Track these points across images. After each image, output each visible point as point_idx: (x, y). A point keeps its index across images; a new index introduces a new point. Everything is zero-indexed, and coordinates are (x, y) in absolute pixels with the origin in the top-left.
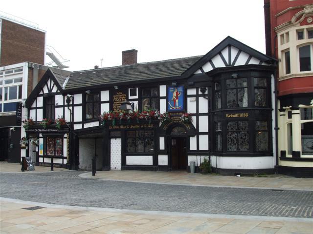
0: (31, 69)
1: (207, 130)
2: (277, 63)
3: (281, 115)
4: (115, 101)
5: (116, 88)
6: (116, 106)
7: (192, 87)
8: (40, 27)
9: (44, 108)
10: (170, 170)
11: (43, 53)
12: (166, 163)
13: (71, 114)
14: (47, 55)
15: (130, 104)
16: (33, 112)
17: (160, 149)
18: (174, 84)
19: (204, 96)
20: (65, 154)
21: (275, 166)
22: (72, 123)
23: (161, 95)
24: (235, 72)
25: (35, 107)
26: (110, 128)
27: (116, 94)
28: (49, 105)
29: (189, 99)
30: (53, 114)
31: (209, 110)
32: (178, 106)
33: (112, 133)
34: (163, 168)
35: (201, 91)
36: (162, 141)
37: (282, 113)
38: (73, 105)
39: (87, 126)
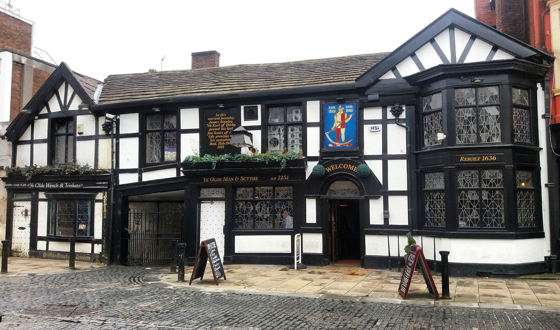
7: (373, 104)
13: (113, 153)
19: (397, 121)
20: (98, 234)
29: (367, 128)
33: (205, 192)
38: (118, 136)
39: (148, 177)
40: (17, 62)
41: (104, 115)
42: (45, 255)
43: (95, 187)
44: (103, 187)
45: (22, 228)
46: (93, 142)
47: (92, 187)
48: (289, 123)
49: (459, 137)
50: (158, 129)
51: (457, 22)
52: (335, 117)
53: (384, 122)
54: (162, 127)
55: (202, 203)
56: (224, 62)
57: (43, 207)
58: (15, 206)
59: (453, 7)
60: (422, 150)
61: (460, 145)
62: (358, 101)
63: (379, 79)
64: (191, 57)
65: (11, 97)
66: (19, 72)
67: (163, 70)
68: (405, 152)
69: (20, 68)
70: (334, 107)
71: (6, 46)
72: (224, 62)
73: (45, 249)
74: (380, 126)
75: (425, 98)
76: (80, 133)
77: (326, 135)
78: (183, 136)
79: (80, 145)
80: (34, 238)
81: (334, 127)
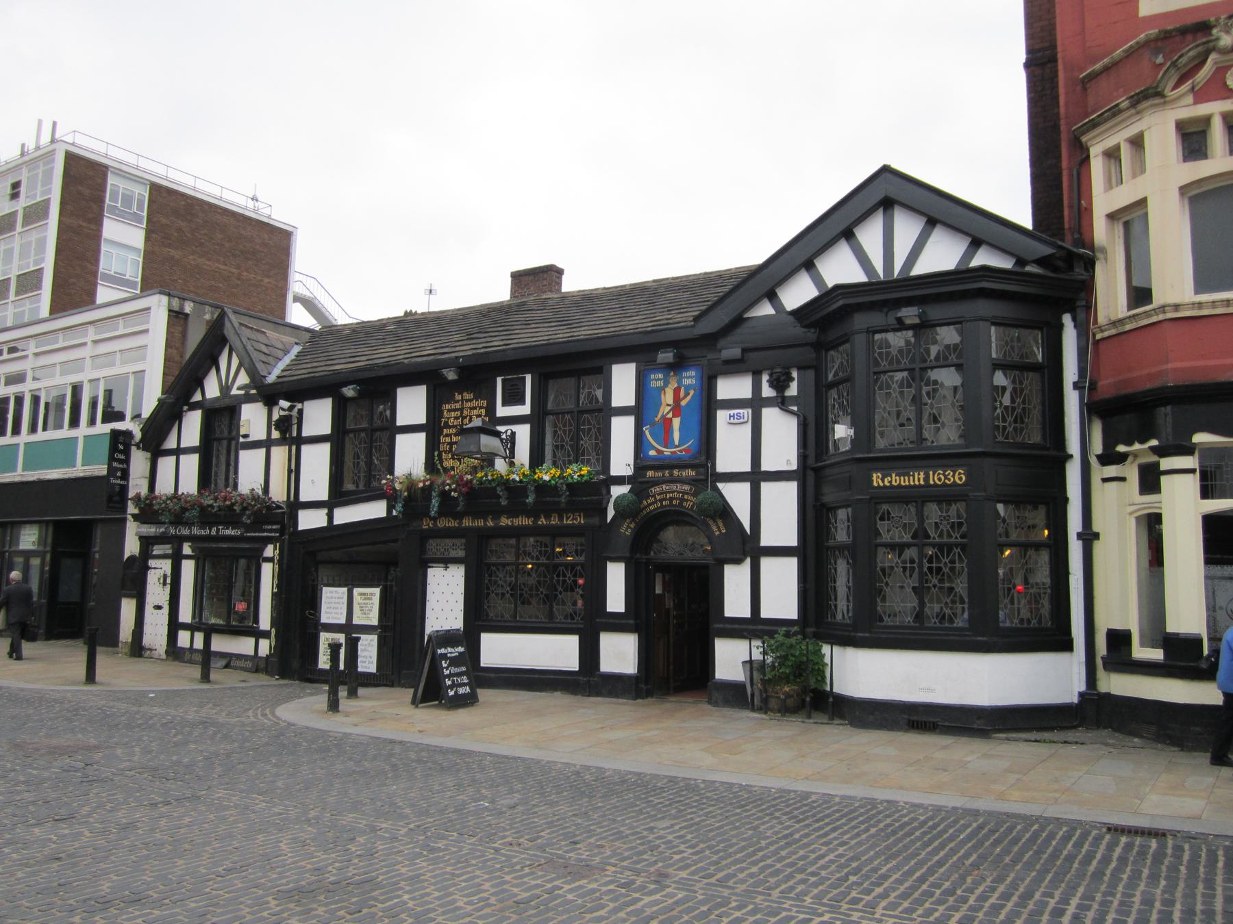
0: (177, 317)
2: (1090, 264)
3: (1105, 480)
4: (447, 426)
5: (451, 375)
6: (451, 444)
7: (733, 368)
8: (279, 215)
9: (206, 450)
10: (648, 694)
11: (284, 296)
13: (290, 471)
14: (298, 304)
15: (497, 434)
16: (166, 465)
17: (609, 609)
18: (666, 356)
19: (782, 402)
20: (265, 623)
21: (1081, 695)
22: (295, 505)
23: (616, 402)
24: (909, 302)
25: (174, 446)
26: (426, 524)
27: (451, 399)
28: (219, 440)
29: (722, 416)
30: (232, 466)
31: (803, 457)
32: (682, 442)
33: (434, 546)
34: (615, 686)
35: (772, 384)
36: (616, 575)
37: (1111, 471)
38: (300, 441)
39: (346, 515)
40: (176, 312)
41: (277, 404)
42: (187, 654)
43: (261, 534)
44: (273, 534)
45: (159, 607)
46: (263, 451)
47: (257, 534)
48: (582, 409)
49: (882, 434)
50: (364, 425)
51: (893, 194)
52: (662, 396)
53: (756, 404)
54: (371, 420)
55: (430, 567)
56: (569, 285)
57: (188, 568)
58: (151, 568)
59: (888, 163)
60: (825, 461)
61: (881, 451)
62: (704, 361)
63: (745, 316)
64: (509, 280)
65: (164, 374)
66: (180, 329)
67: (431, 310)
68: (794, 467)
69: (182, 322)
70: (661, 376)
71: (245, 274)
72: (569, 285)
73: (188, 645)
74: (747, 413)
75: (832, 353)
76: (246, 436)
78: (401, 439)
79: (244, 455)
80: (174, 625)
81: (659, 416)
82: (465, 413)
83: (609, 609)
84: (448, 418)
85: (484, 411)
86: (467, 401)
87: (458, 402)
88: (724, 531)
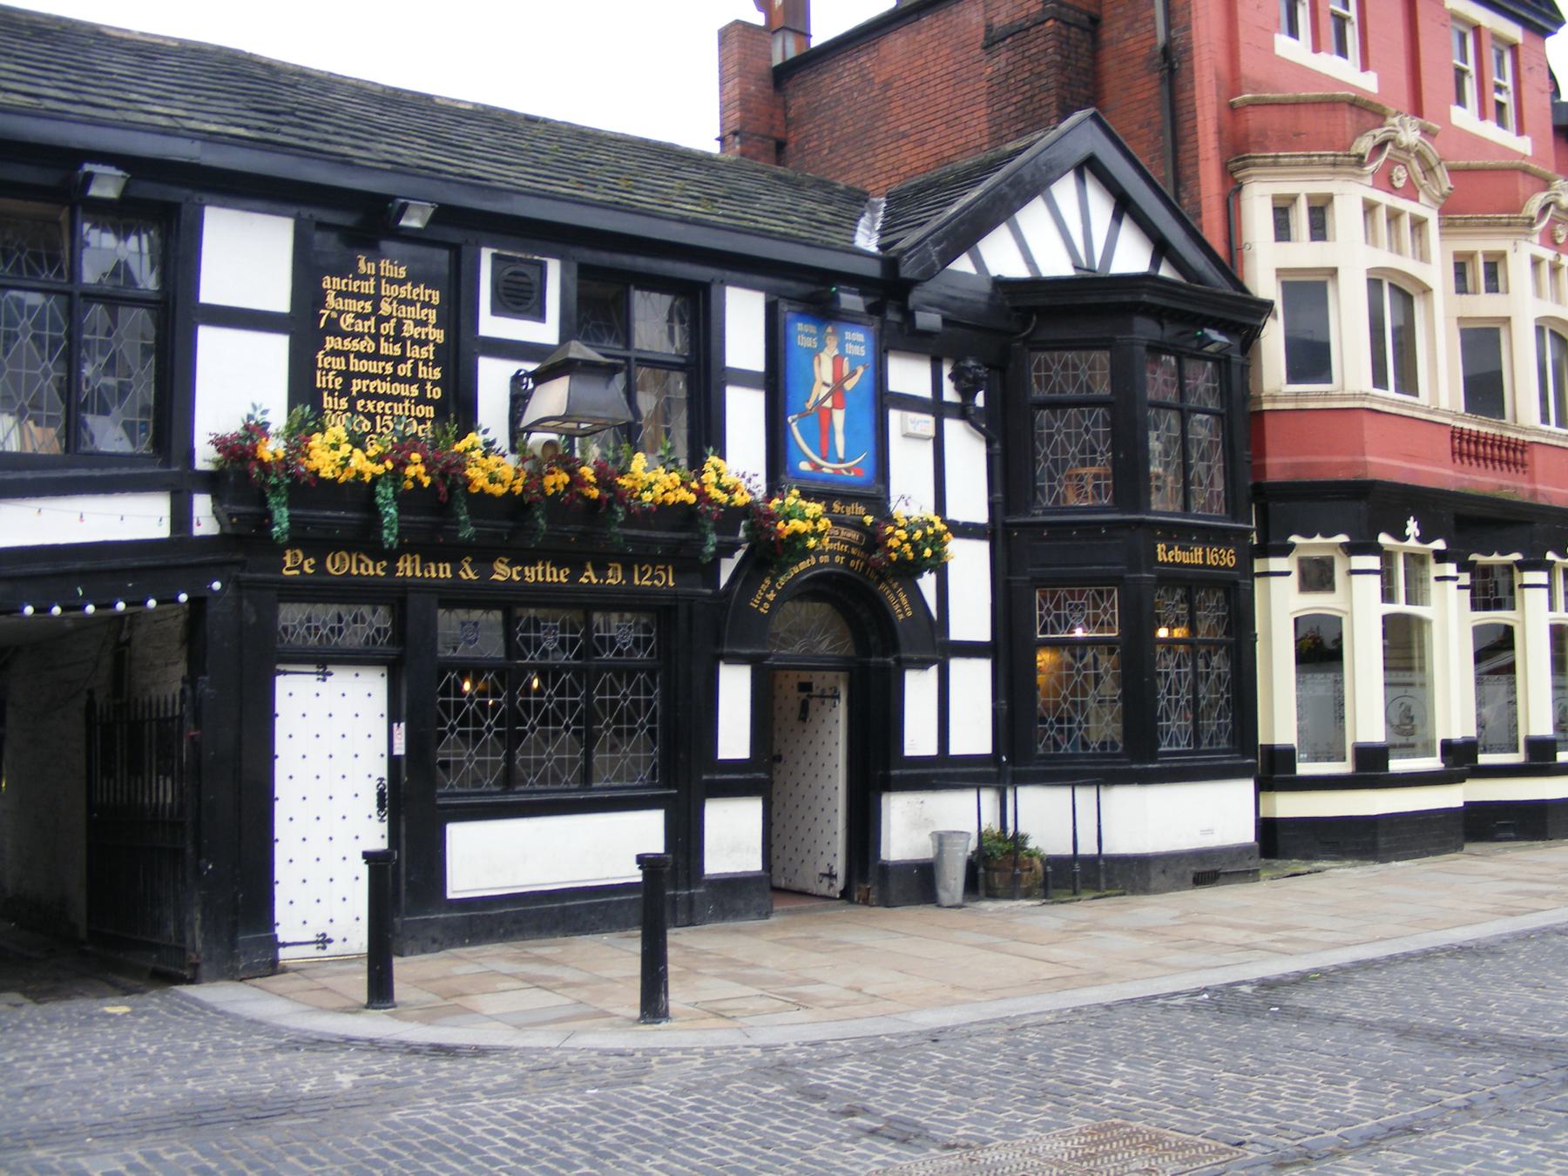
1: (982, 633)
4: (334, 328)
6: (348, 376)
12: (749, 860)
17: (908, 752)
19: (963, 412)
55: (285, 673)
60: (1034, 515)
77: (790, 425)
82: (385, 309)
83: (908, 752)
84: (340, 313)
85: (433, 316)
86: (391, 281)
87: (366, 277)
88: (909, 614)
